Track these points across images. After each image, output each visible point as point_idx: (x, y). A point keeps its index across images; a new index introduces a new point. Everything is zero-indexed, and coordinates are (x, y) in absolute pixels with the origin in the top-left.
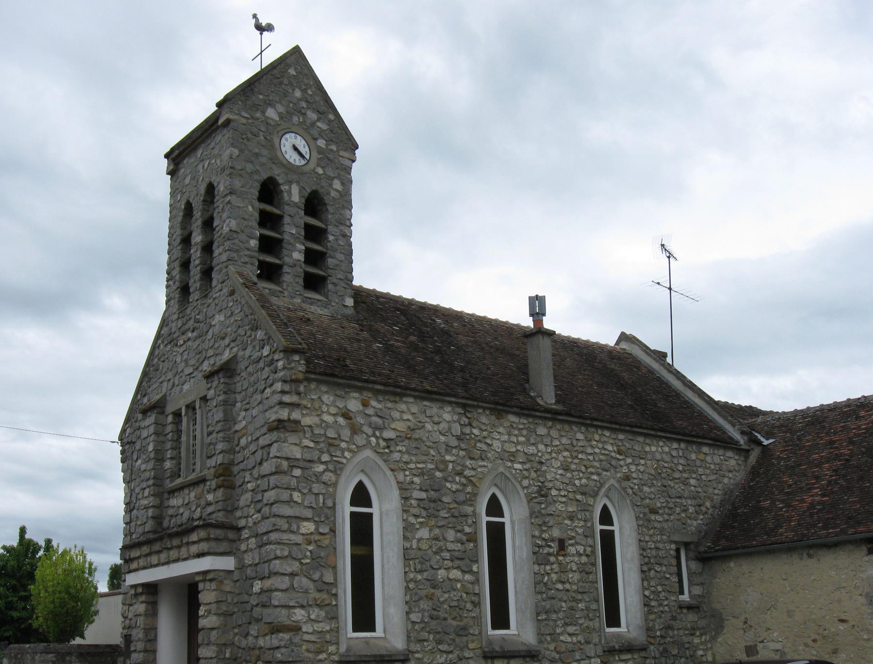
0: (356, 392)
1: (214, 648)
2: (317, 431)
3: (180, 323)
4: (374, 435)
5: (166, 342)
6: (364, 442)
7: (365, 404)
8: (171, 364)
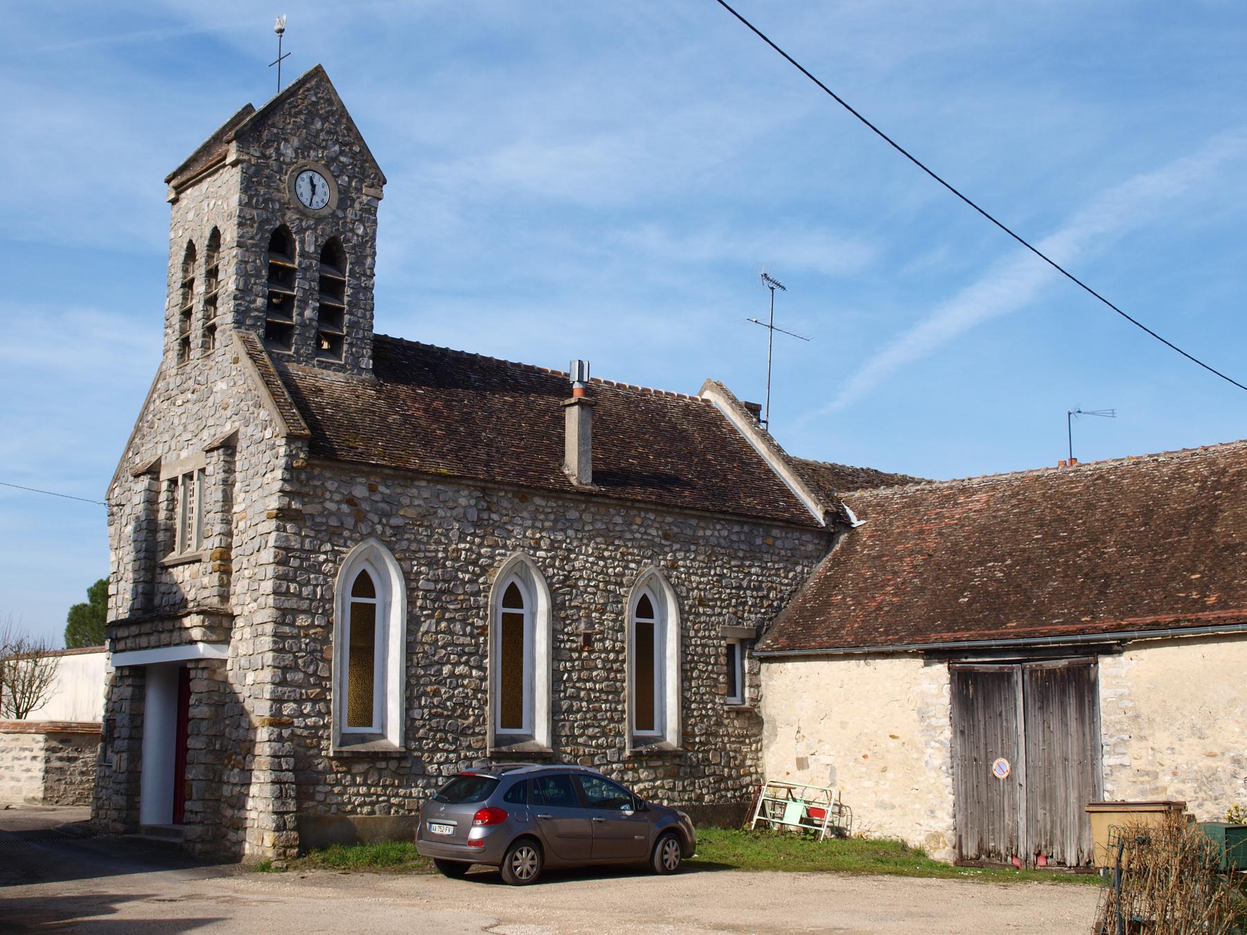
0: (363, 477)
1: (203, 739)
2: (318, 520)
3: (178, 382)
4: (380, 522)
6: (369, 530)
7: (372, 489)
8: (168, 424)
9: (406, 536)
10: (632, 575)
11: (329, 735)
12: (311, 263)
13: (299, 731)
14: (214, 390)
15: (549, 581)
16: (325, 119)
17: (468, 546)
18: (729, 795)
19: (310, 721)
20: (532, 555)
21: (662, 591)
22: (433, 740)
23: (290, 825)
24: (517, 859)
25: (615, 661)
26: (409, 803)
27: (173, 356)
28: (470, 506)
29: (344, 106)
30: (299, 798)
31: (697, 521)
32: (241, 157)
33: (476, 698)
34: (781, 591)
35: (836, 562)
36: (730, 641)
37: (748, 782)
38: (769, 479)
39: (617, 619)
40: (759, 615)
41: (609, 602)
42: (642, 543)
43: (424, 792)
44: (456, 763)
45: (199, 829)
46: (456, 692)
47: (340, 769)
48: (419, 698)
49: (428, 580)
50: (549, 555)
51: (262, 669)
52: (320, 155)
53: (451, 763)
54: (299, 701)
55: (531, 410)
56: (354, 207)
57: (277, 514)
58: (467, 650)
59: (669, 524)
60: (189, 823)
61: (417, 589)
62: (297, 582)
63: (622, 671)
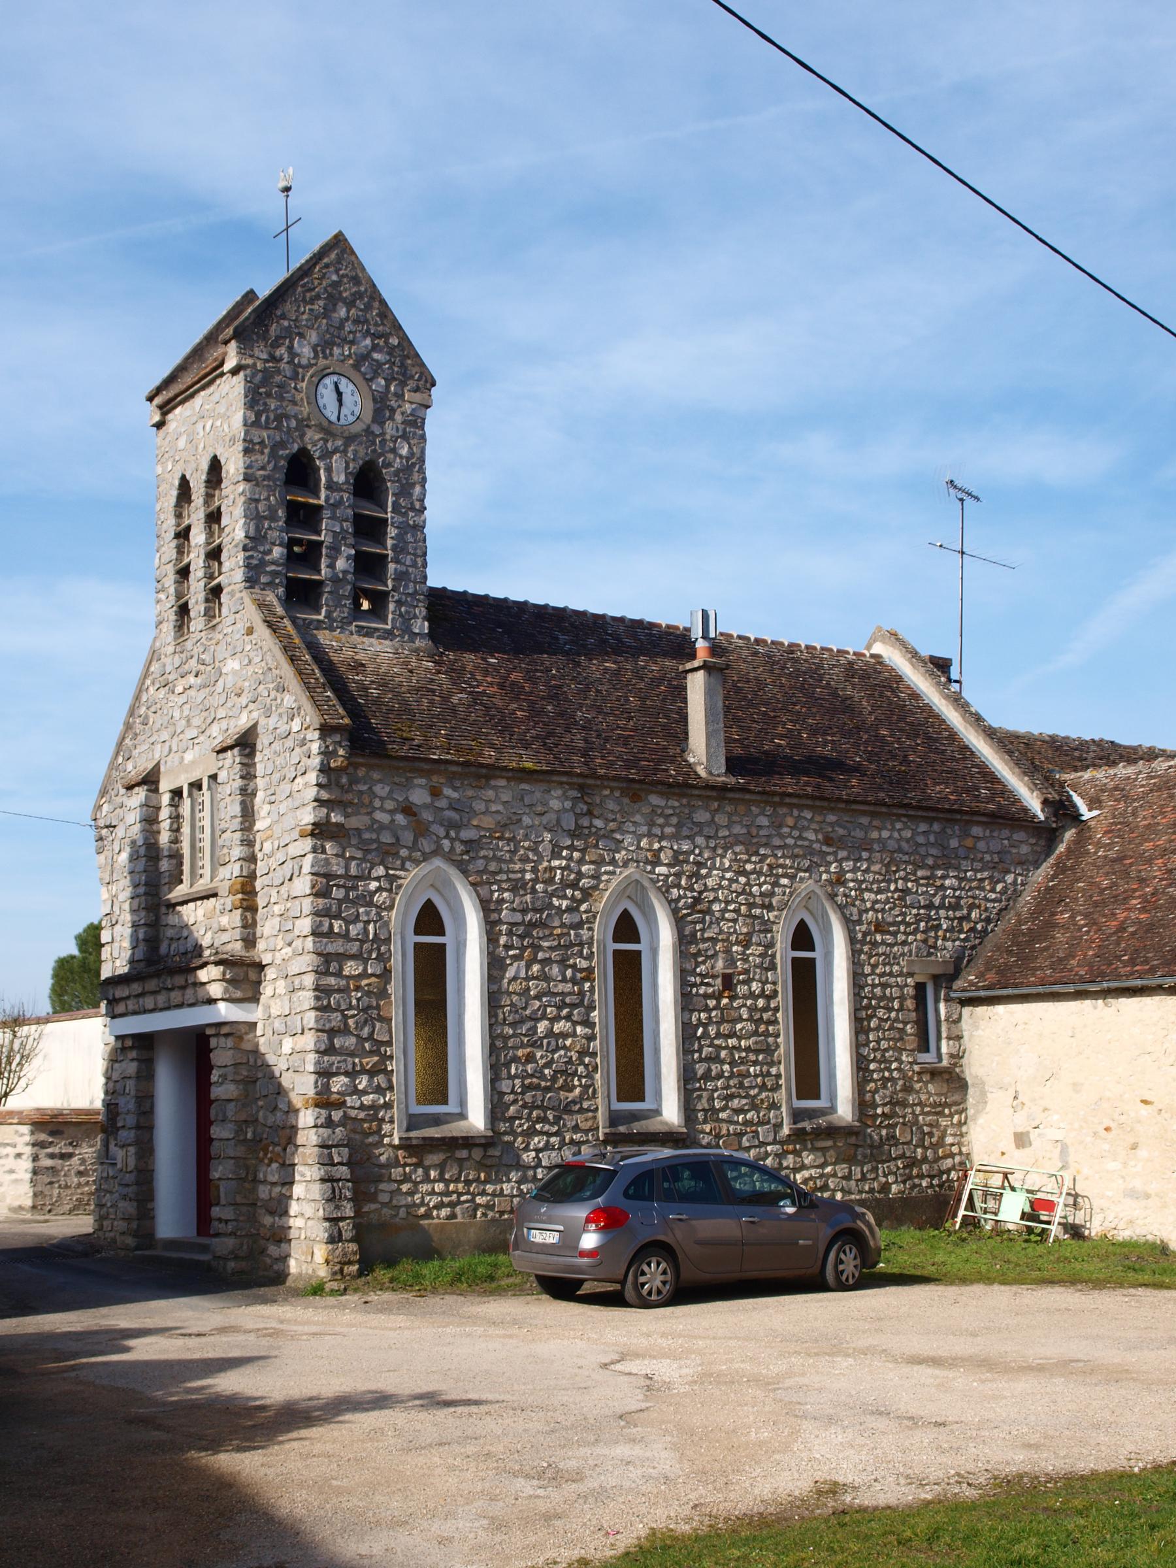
0: (421, 777)
2: (367, 836)
3: (177, 660)
4: (447, 836)
5: (157, 686)
6: (433, 847)
7: (435, 793)
8: (167, 718)
9: (482, 853)
10: (784, 894)
11: (392, 1117)
12: (342, 497)
13: (353, 1113)
14: (224, 671)
15: (673, 905)
16: (350, 304)
17: (564, 863)
18: (924, 1184)
19: (367, 1100)
20: (650, 872)
21: (825, 915)
22: (529, 1119)
23: (347, 1235)
24: (643, 1273)
25: (766, 1009)
26: (500, 1203)
27: (168, 628)
28: (565, 810)
29: (374, 285)
30: (359, 1199)
31: (869, 819)
32: (243, 362)
33: (582, 1063)
34: (986, 909)
35: (1060, 868)
36: (920, 979)
37: (950, 1165)
38: (965, 759)
39: (766, 952)
40: (957, 943)
41: (754, 931)
42: (796, 851)
43: (519, 1188)
44: (560, 1149)
45: (230, 1242)
46: (556, 1056)
47: (409, 1161)
48: (507, 1065)
49: (514, 910)
50: (672, 871)
51: (302, 1034)
52: (347, 353)
53: (553, 1149)
54: (352, 1074)
55: (642, 679)
56: (393, 420)
57: (313, 830)
58: (568, 1000)
59: (832, 824)
60: (217, 1235)
61: (499, 922)
62: (343, 919)
63: (775, 1022)
